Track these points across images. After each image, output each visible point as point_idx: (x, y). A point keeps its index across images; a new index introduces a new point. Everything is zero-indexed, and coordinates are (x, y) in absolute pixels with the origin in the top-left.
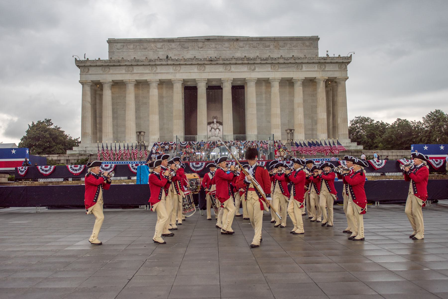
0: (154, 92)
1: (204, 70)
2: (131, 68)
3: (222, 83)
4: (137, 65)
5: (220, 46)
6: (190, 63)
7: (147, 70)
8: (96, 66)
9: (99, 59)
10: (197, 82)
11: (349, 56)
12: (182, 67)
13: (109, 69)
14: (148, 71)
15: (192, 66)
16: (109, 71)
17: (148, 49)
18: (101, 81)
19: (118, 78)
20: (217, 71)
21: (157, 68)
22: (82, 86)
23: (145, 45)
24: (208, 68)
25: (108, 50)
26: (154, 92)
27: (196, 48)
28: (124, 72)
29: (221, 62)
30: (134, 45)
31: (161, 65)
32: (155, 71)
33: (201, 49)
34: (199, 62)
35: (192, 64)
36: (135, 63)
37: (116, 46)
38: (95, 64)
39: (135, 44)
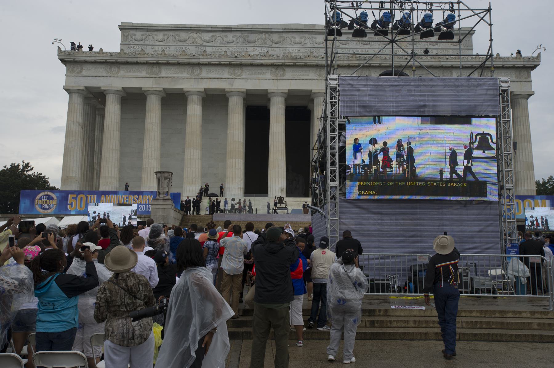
0: (194, 110)
1: (284, 75)
2: (155, 69)
3: (313, 101)
4: (168, 64)
5: (308, 41)
6: (259, 61)
7: (184, 73)
9: (101, 49)
10: (269, 96)
11: (535, 55)
12: (245, 69)
13: (119, 68)
14: (185, 75)
15: (262, 68)
16: (118, 72)
17: (188, 42)
18: (102, 89)
20: (305, 77)
21: (201, 70)
22: (68, 95)
23: (183, 35)
24: (289, 73)
25: (120, 42)
26: (194, 110)
27: (269, 43)
29: (313, 62)
30: (164, 35)
31: (209, 65)
32: (198, 75)
33: (277, 45)
34: (275, 61)
35: (262, 65)
36: (164, 60)
37: (135, 35)
39: (166, 33)
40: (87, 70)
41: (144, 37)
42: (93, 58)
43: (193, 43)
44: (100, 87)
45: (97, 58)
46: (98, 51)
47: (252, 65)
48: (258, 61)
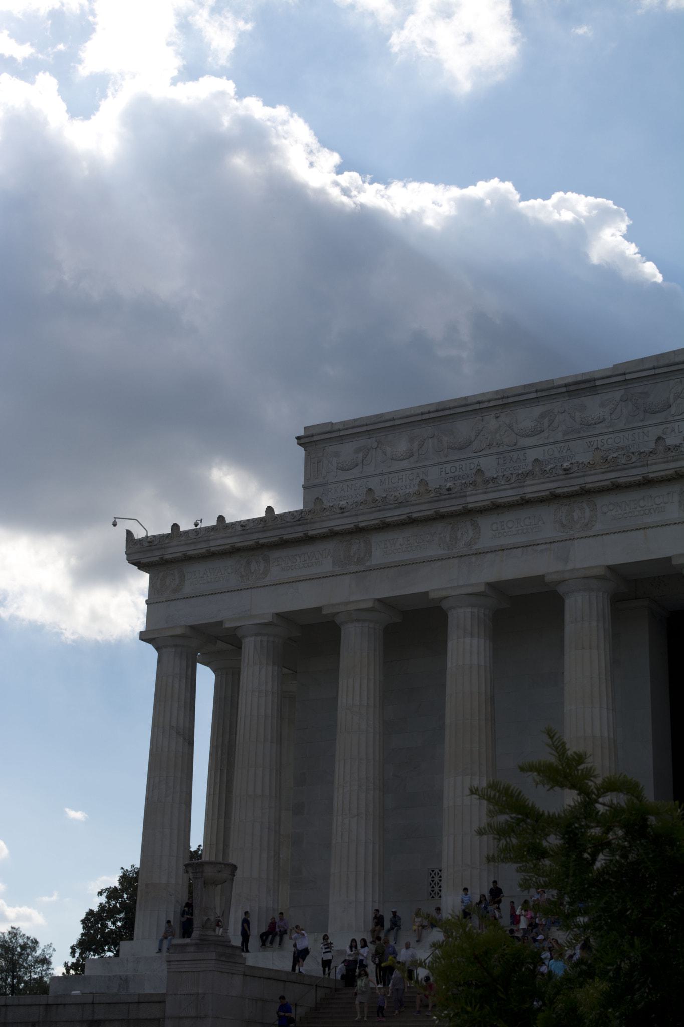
0: (466, 651)
4: (384, 526)
8: (210, 555)
18: (227, 625)
19: (303, 598)
22: (155, 654)
23: (464, 428)
26: (466, 651)
28: (327, 566)
31: (495, 508)
38: (200, 548)
40: (199, 577)
41: (361, 455)
42: (203, 545)
43: (490, 446)
44: (221, 623)
45: (212, 543)
46: (214, 523)
47: (616, 488)
48: (635, 472)
